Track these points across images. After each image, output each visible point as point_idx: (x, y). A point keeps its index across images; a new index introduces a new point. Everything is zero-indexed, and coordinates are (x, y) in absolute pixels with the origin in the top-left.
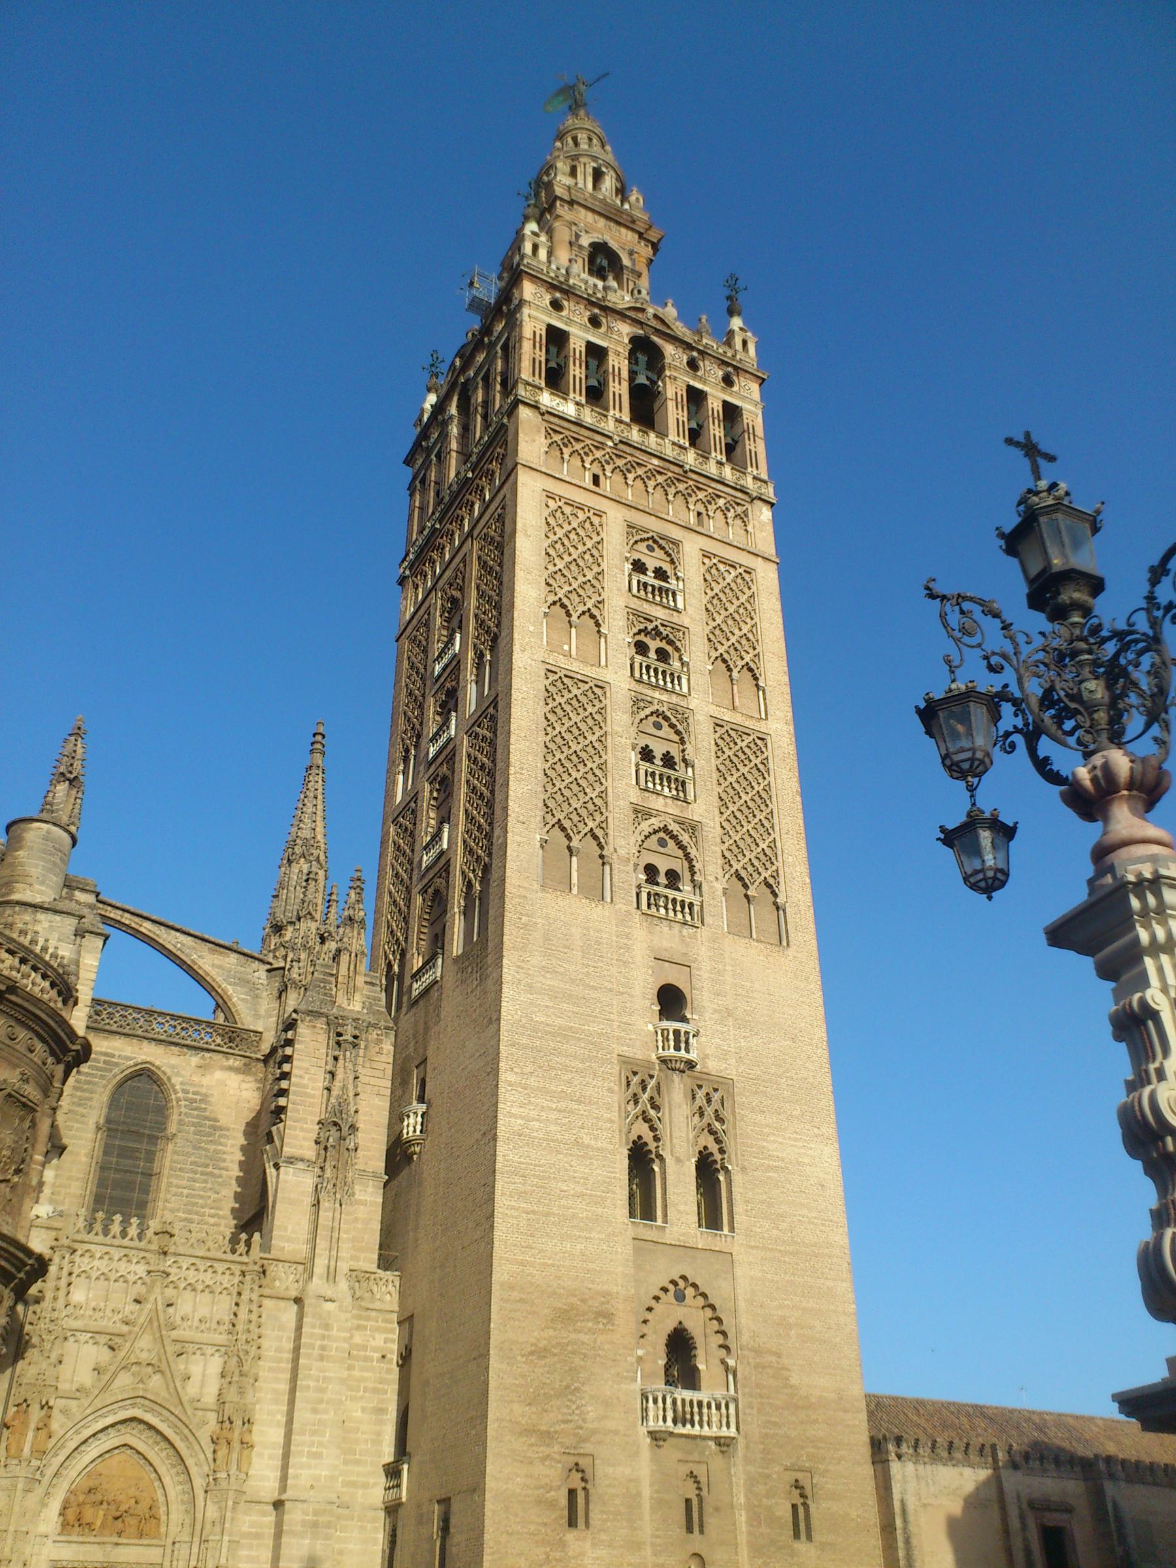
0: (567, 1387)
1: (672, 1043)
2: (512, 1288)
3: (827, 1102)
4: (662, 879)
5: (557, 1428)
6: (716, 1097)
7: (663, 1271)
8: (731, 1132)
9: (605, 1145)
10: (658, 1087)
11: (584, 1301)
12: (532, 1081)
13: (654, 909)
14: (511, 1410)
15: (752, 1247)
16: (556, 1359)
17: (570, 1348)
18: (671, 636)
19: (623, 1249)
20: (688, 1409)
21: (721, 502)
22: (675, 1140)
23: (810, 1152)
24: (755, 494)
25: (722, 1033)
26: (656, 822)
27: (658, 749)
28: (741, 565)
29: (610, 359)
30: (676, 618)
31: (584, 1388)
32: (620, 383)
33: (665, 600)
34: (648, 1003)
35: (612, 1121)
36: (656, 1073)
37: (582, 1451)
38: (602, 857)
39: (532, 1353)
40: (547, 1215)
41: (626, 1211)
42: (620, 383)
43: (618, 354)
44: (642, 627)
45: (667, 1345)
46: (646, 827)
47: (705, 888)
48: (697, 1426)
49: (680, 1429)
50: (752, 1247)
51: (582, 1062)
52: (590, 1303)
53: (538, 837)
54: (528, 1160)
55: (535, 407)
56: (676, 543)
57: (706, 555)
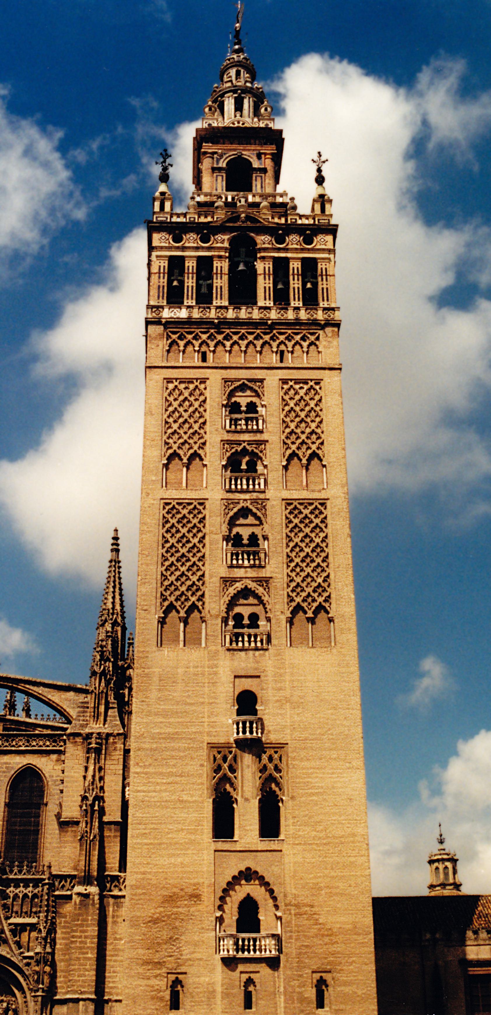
0: (170, 938)
1: (241, 730)
2: (138, 888)
3: (358, 744)
4: (246, 621)
5: (165, 960)
6: (276, 756)
7: (234, 866)
8: (285, 778)
9: (197, 798)
10: (235, 758)
11: (182, 890)
12: (151, 770)
13: (234, 645)
14: (137, 953)
15: (297, 844)
16: (164, 923)
17: (173, 916)
18: (255, 450)
19: (208, 856)
20: (246, 943)
21: (298, 338)
22: (244, 788)
23: (341, 780)
24: (323, 322)
25: (281, 714)
26: (239, 586)
27: (245, 533)
28: (311, 380)
29: (215, 262)
30: (258, 437)
31: (182, 938)
32: (221, 278)
33: (250, 427)
34: (229, 706)
35: (202, 784)
36: (234, 750)
37: (179, 971)
38: (201, 618)
39: (149, 922)
40: (160, 844)
41: (211, 835)
42: (221, 278)
43: (220, 257)
44: (233, 450)
45: (238, 908)
46: (231, 591)
47: (273, 621)
48: (252, 953)
49: (240, 955)
50: (297, 844)
51: (184, 752)
52: (186, 890)
53: (157, 616)
54: (148, 815)
55: (158, 322)
56: (262, 381)
57: (284, 381)
